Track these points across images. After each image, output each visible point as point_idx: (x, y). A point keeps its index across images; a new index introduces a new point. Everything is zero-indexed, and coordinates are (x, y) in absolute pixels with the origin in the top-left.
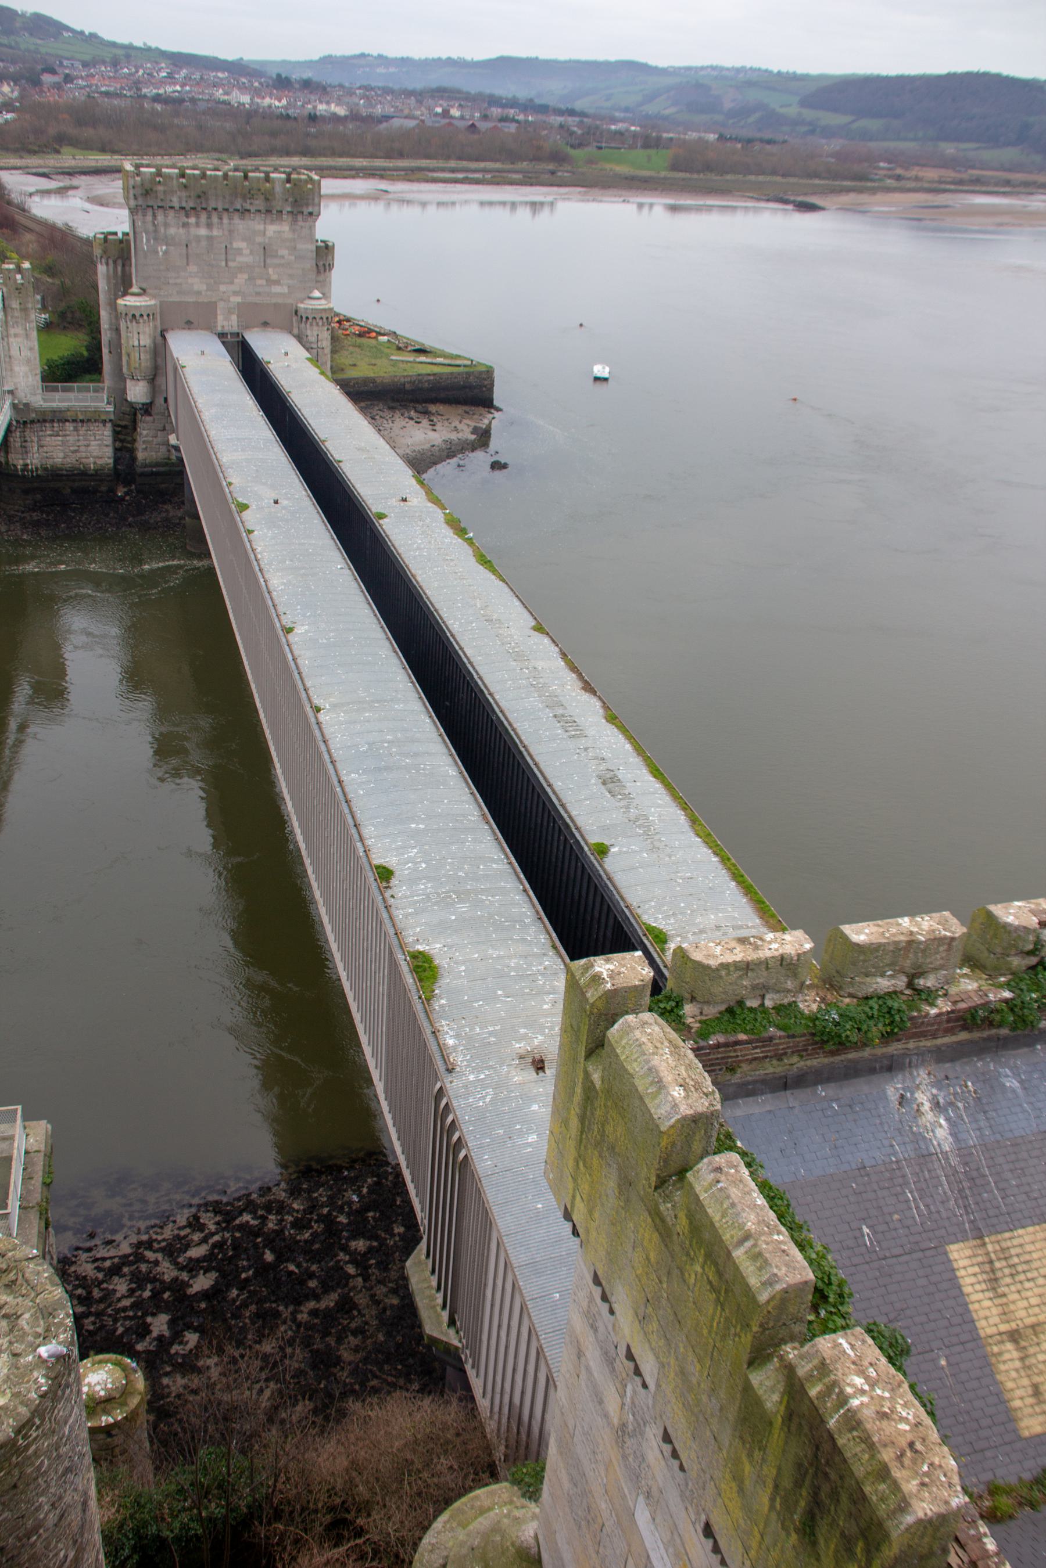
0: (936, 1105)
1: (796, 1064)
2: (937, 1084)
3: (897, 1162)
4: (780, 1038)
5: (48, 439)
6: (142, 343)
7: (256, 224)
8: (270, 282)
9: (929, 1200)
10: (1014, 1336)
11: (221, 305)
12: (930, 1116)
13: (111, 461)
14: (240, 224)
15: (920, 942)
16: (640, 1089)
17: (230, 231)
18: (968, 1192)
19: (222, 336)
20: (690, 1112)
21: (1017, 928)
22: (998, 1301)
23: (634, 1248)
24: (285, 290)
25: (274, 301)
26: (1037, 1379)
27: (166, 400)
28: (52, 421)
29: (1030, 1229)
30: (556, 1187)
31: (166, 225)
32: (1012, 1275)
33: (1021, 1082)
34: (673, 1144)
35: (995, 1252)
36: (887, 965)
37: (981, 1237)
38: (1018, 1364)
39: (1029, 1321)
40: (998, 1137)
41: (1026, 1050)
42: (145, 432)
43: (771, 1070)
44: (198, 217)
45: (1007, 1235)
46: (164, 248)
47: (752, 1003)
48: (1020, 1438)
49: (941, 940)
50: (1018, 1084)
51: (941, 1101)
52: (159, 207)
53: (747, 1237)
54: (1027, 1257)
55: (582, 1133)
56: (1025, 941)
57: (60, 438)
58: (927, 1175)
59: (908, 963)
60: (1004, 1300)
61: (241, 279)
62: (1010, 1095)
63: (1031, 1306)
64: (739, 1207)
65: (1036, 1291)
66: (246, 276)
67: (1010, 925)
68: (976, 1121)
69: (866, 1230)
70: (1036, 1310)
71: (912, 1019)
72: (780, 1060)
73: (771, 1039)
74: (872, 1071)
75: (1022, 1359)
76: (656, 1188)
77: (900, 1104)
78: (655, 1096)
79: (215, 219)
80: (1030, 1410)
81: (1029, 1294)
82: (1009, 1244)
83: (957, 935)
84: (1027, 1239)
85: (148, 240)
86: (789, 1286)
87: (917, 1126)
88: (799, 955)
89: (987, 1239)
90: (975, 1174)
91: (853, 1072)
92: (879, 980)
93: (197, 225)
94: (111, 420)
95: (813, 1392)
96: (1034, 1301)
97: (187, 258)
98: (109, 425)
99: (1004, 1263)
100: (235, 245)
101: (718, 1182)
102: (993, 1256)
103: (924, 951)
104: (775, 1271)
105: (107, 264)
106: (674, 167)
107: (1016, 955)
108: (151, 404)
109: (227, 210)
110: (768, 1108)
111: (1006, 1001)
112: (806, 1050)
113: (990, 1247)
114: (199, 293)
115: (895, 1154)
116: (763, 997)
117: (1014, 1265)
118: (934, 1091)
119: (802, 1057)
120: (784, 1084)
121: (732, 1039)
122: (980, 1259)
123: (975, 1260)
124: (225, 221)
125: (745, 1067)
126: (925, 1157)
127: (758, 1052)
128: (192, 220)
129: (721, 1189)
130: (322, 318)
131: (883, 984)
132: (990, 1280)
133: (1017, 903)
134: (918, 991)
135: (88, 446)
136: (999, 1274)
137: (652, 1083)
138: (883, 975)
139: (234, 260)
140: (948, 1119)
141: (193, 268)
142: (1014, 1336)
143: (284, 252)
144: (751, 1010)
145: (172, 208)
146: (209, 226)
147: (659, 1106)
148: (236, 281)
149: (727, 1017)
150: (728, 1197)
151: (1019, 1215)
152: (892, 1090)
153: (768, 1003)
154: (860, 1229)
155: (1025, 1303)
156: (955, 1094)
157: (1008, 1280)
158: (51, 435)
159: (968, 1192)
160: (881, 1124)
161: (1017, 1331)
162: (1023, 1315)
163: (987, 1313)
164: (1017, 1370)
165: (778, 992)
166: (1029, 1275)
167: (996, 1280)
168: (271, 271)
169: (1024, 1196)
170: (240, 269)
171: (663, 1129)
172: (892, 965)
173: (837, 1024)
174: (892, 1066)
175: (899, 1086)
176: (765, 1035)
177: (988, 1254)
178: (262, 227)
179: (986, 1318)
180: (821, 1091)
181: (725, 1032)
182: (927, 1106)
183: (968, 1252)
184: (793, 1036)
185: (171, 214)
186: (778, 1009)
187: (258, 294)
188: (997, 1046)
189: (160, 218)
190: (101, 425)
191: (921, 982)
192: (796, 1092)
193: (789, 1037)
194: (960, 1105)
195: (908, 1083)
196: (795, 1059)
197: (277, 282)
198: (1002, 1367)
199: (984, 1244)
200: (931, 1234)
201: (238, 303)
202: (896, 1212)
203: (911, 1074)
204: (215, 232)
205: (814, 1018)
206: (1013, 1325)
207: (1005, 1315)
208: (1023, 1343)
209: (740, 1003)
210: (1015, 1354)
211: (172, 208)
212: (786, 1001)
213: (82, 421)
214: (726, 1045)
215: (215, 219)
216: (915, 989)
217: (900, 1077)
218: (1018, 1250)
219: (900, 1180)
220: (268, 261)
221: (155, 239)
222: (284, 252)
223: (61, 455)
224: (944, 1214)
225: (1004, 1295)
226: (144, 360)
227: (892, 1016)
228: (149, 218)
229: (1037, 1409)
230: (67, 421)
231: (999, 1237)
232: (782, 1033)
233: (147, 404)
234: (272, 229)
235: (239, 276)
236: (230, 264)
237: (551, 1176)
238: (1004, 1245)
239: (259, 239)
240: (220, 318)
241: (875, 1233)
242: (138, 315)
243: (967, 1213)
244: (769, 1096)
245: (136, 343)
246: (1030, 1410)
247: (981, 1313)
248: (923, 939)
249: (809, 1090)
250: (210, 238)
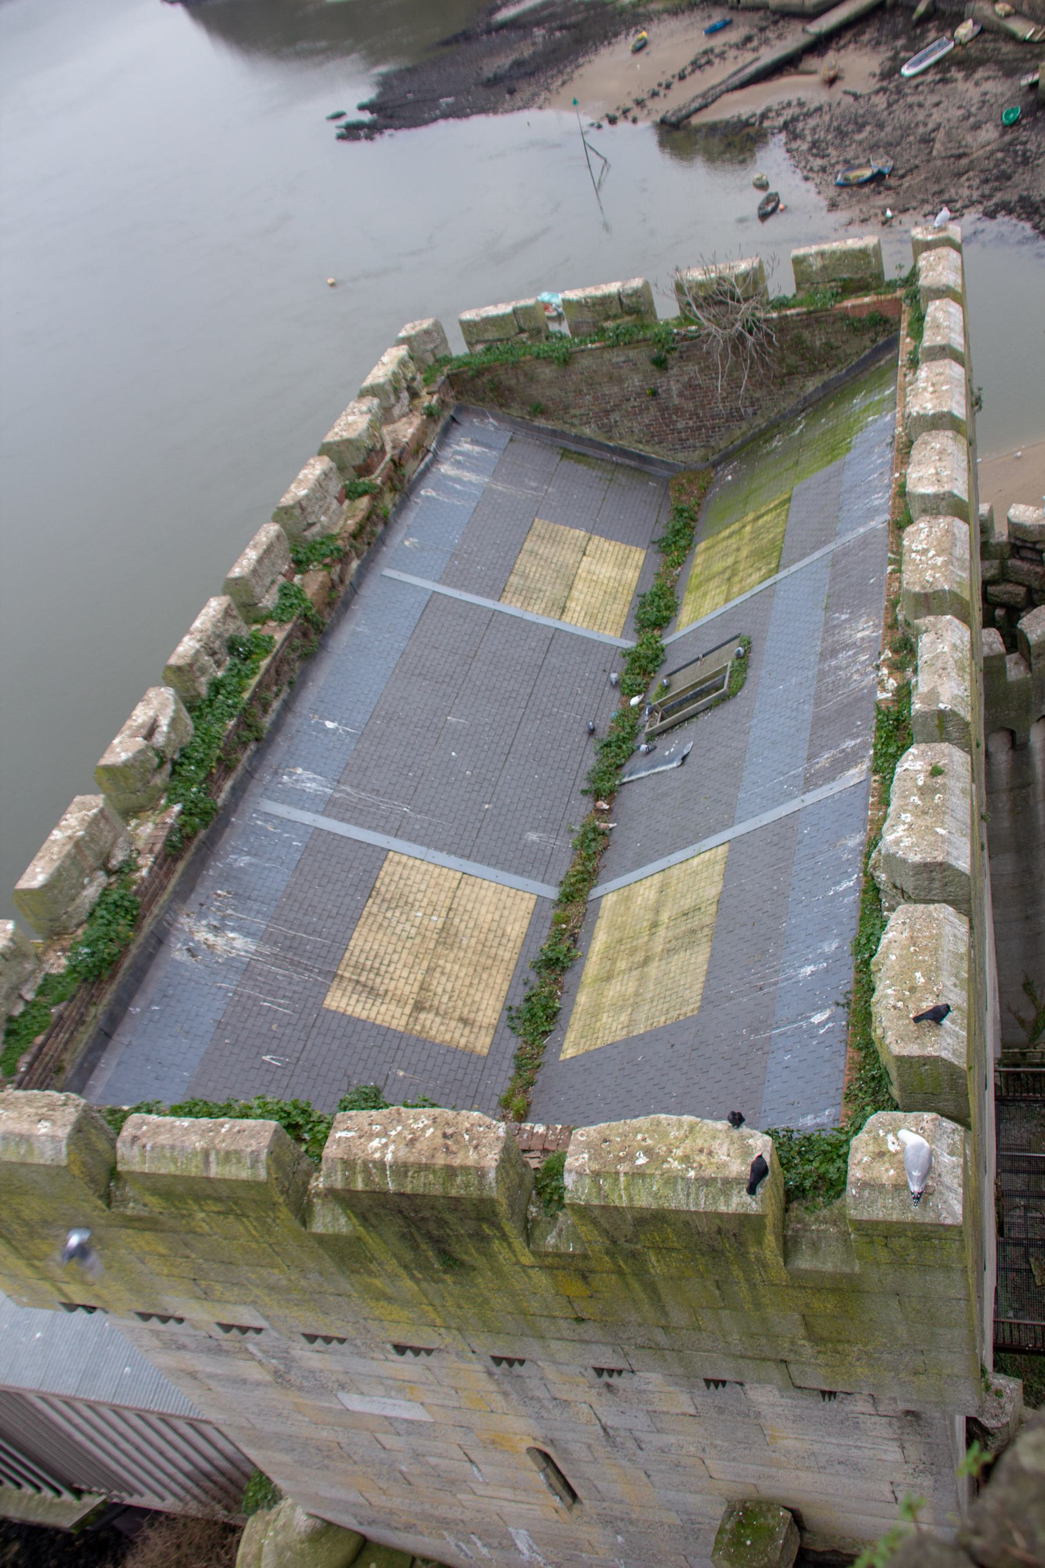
0: (216, 930)
1: (97, 1012)
2: (201, 916)
3: (235, 993)
4: (66, 1009)
9: (281, 992)
10: (419, 1007)
12: (220, 942)
15: (83, 838)
16: (14, 1159)
18: (296, 958)
20: (68, 1129)
21: (134, 758)
22: (387, 1000)
23: (142, 1262)
26: (457, 1015)
29: (356, 935)
30: (39, 1301)
32: (377, 974)
33: (248, 854)
34: (84, 1164)
35: (353, 973)
36: (79, 876)
37: (335, 975)
38: (438, 1020)
39: (416, 989)
40: (274, 903)
41: (228, 830)
43: (85, 1037)
45: (347, 955)
47: (19, 1009)
48: (486, 1058)
49: (95, 821)
50: (247, 858)
51: (215, 923)
53: (206, 1154)
54: (373, 953)
55: (9, 1242)
56: (149, 760)
58: (262, 979)
59: (91, 860)
60: (390, 994)
62: (251, 870)
63: (407, 978)
64: (178, 1144)
65: (400, 966)
67: (128, 760)
68: (250, 910)
69: (267, 1058)
70: (412, 976)
71: (136, 893)
72: (83, 1023)
73: (61, 1017)
74: (151, 957)
75: (437, 1014)
76: (109, 1205)
77: (193, 956)
78: (30, 1150)
80: (473, 1036)
81: (398, 972)
82: (354, 959)
83: (101, 805)
84: (361, 943)
86: (269, 1146)
87: (220, 956)
88: (11, 940)
89: (340, 972)
90: (288, 943)
91: (140, 973)
92: (85, 893)
95: (360, 1186)
96: (405, 974)
99: (365, 973)
101: (144, 1146)
102: (354, 977)
103: (92, 840)
104: (249, 1150)
107: (153, 776)
110: (114, 1063)
111: (182, 813)
112: (93, 996)
113: (347, 975)
115: (228, 990)
116: (21, 997)
117: (372, 967)
118: (204, 922)
119: (95, 1004)
120: (106, 1035)
121: (34, 1049)
122: (350, 989)
123: (348, 993)
125: (66, 1056)
126: (247, 969)
127: (63, 1036)
129: (153, 1148)
131: (91, 892)
132: (369, 993)
133: (116, 741)
134: (119, 871)
136: (370, 983)
137: (18, 1145)
138: (84, 887)
140: (233, 930)
142: (419, 1007)
144: (23, 1015)
147: (42, 1153)
149: (12, 1040)
150: (163, 1147)
151: (340, 935)
152: (178, 953)
153: (30, 996)
154: (264, 1062)
155: (402, 981)
156: (219, 909)
157: (379, 980)
159: (296, 958)
160: (197, 983)
161: (416, 1002)
162: (409, 989)
163: (390, 1013)
164: (442, 1024)
165: (26, 981)
166: (386, 962)
167: (372, 988)
169: (330, 920)
171: (64, 1163)
172: (82, 873)
173: (92, 954)
174: (160, 939)
175: (179, 945)
176: (53, 1019)
177: (350, 980)
179: (393, 1017)
180: (135, 1010)
181: (24, 1051)
182: (211, 938)
183: (339, 993)
184: (74, 997)
186: (41, 991)
188: (209, 846)
191: (114, 863)
192: (119, 1030)
193: (71, 1001)
194: (229, 912)
195: (182, 937)
196: (93, 1010)
198: (433, 1033)
199: (342, 977)
200: (307, 1011)
202: (271, 1024)
203: (177, 929)
205: (73, 969)
206: (411, 1002)
207: (400, 1001)
208: (427, 1005)
209: (10, 1019)
210: (431, 1016)
212: (40, 981)
214: (36, 1058)
216: (115, 872)
217: (173, 939)
218: (364, 956)
219: (250, 1002)
224: (298, 989)
225: (387, 991)
227: (121, 906)
229: (476, 1030)
231: (344, 962)
232: (62, 1006)
237: (25, 1299)
238: (352, 963)
241: (274, 1053)
243: (311, 971)
244: (105, 1055)
246: (473, 1036)
247: (388, 1018)
248: (81, 833)
249: (127, 1019)
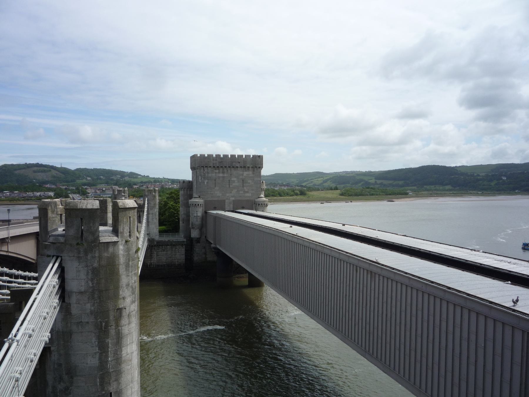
5: (160, 252)
6: (198, 215)
7: (240, 171)
8: (245, 192)
11: (227, 201)
13: (184, 261)
14: (234, 172)
17: (230, 174)
24: (250, 195)
25: (246, 199)
27: (206, 237)
28: (162, 246)
31: (208, 173)
42: (197, 250)
44: (219, 169)
46: (207, 181)
52: (206, 167)
57: (165, 252)
61: (235, 191)
66: (236, 190)
79: (225, 170)
85: (201, 179)
93: (219, 173)
94: (185, 244)
97: (215, 184)
98: (184, 246)
100: (232, 179)
105: (184, 190)
106: (342, 194)
108: (200, 238)
109: (229, 167)
114: (219, 197)
124: (229, 171)
128: (217, 171)
130: (264, 204)
135: (175, 255)
141: (217, 188)
143: (250, 181)
145: (210, 167)
146: (223, 173)
148: (232, 192)
158: (161, 251)
168: (245, 188)
178: (242, 173)
185: (210, 169)
187: (240, 196)
189: (206, 170)
190: (181, 246)
197: (247, 192)
204: (225, 175)
211: (210, 167)
213: (174, 245)
215: (225, 170)
220: (244, 185)
221: (204, 178)
222: (250, 181)
223: (165, 259)
226: (198, 222)
228: (202, 171)
230: (168, 245)
233: (198, 238)
234: (245, 173)
236: (230, 186)
239: (241, 177)
240: (226, 206)
242: (197, 204)
245: (196, 215)
250: (223, 177)
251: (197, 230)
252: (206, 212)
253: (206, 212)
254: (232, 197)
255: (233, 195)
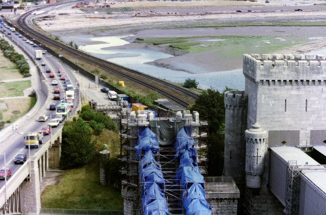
11: (302, 132)
19: (303, 149)
27: (268, 186)
61: (313, 117)
93: (292, 89)
98: (236, 201)
100: (311, 99)
105: (234, 110)
114: (290, 126)
139: (310, 108)
148: (310, 118)
170: (313, 112)
201: (312, 131)
233: (258, 188)
235: (313, 116)
236: (308, 109)
250: (298, 96)
251: (256, 177)
252: (269, 150)
253: (269, 150)
254: (310, 125)
255: (311, 123)
